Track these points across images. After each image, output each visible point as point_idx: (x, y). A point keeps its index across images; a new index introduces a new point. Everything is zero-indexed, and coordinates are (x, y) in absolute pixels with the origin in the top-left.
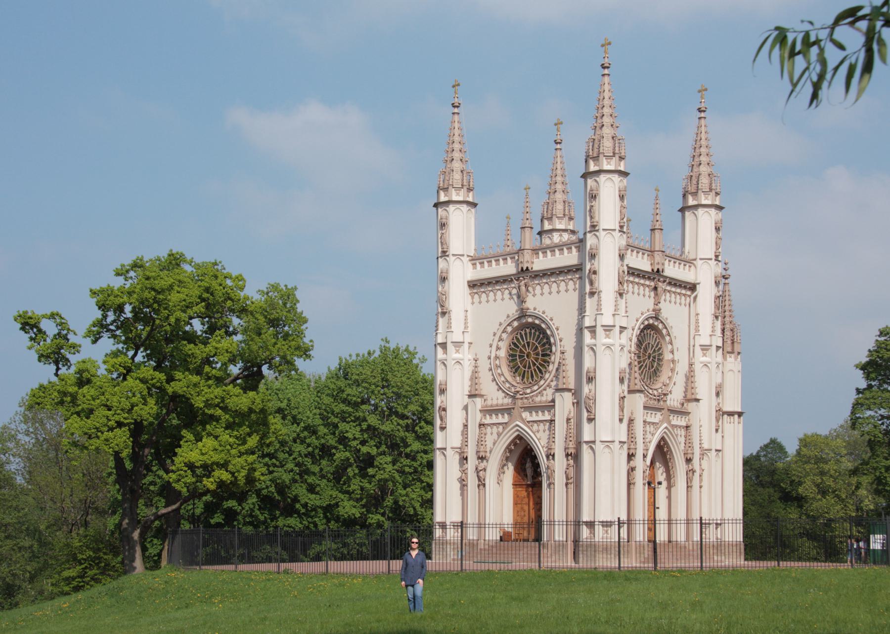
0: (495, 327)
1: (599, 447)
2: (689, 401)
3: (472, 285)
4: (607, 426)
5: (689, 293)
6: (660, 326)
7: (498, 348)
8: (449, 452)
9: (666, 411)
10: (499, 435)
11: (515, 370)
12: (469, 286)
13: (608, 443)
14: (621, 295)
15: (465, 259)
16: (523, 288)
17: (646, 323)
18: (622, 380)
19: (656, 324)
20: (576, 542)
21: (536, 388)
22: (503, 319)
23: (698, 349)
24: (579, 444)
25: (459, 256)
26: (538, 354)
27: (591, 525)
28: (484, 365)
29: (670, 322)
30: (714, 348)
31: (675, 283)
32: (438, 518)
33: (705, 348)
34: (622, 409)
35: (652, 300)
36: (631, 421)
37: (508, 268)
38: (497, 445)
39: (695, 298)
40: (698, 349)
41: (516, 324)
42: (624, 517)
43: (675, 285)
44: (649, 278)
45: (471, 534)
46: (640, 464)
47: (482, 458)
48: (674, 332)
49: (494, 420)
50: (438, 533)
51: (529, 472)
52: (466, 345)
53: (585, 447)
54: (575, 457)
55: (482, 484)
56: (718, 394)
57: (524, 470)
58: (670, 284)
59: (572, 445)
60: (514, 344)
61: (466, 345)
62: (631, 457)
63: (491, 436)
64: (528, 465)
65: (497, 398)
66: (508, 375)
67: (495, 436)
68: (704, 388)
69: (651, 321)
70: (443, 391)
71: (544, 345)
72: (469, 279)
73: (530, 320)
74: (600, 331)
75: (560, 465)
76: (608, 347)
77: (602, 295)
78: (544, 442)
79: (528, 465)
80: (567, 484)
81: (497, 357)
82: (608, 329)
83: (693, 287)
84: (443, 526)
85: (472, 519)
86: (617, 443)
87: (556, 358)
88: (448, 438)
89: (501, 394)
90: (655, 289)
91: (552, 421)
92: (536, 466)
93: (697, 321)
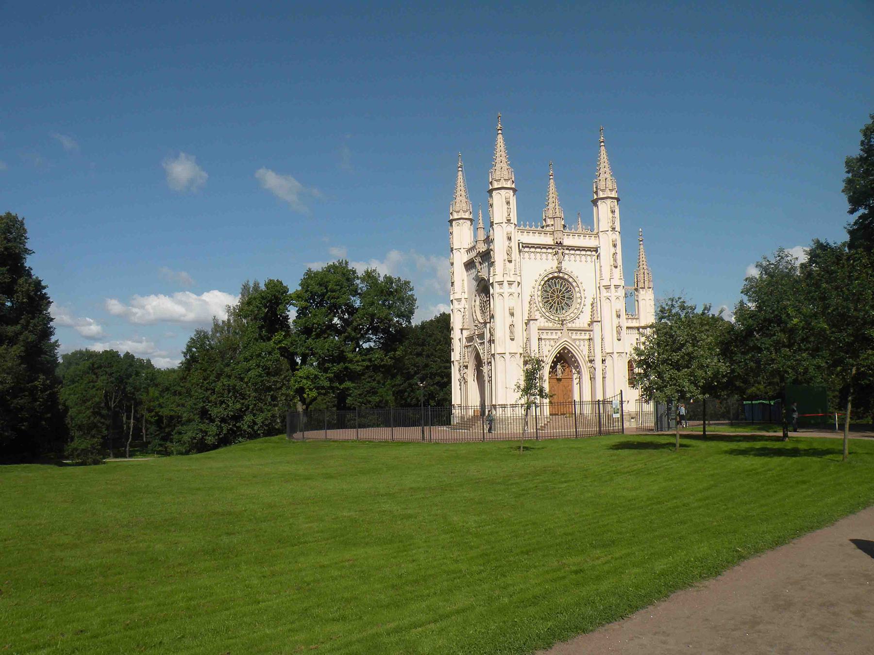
1: (497, 357)
5: (594, 253)
6: (566, 277)
8: (455, 363)
9: (565, 331)
17: (551, 276)
19: (561, 275)
23: (602, 288)
29: (574, 275)
33: (607, 287)
35: (556, 262)
40: (602, 288)
48: (580, 279)
52: (463, 300)
55: (466, 382)
69: (556, 275)
72: (465, 260)
74: (506, 284)
77: (496, 263)
82: (501, 283)
86: (507, 354)
88: (455, 356)
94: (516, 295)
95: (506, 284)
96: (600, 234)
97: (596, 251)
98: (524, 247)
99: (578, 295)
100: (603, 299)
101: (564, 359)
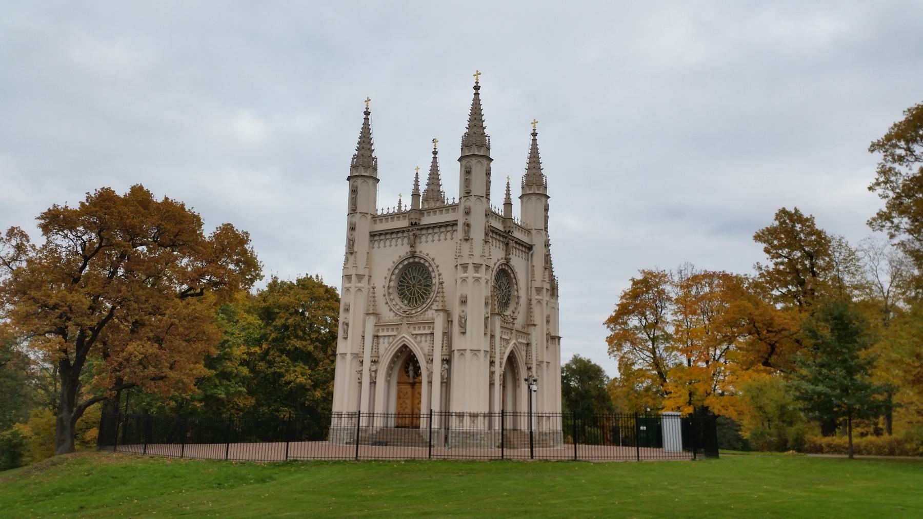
0: (390, 265)
1: (468, 354)
2: (528, 325)
3: (373, 235)
4: (474, 339)
7: (390, 281)
8: (349, 357)
10: (390, 344)
11: (402, 295)
12: (371, 236)
13: (475, 352)
14: (486, 242)
15: (369, 217)
16: (412, 237)
18: (486, 304)
20: (447, 429)
21: (419, 309)
22: (396, 259)
24: (451, 352)
25: (364, 214)
26: (421, 285)
27: (460, 415)
28: (380, 291)
30: (545, 290)
31: (519, 243)
32: (336, 408)
33: (539, 290)
34: (486, 327)
36: (492, 336)
37: (404, 223)
38: (387, 350)
39: (532, 255)
40: (533, 289)
41: (406, 263)
42: (487, 411)
43: (519, 244)
44: (503, 236)
45: (364, 423)
46: (498, 370)
47: (374, 362)
49: (385, 333)
50: (334, 421)
51: (411, 373)
53: (456, 355)
54: (447, 361)
55: (373, 383)
56: (548, 322)
57: (407, 372)
58: (516, 242)
59: (445, 352)
60: (404, 278)
61: (366, 278)
62: (492, 363)
63: (383, 345)
64: (411, 368)
65: (388, 316)
66: (398, 300)
67: (386, 345)
68: (538, 318)
70: (347, 310)
71: (426, 278)
73: (417, 260)
74: (471, 267)
75: (437, 368)
76: (477, 280)
78: (426, 351)
79: (411, 368)
80: (442, 383)
81: (389, 287)
82: (477, 267)
83: (530, 248)
84: (340, 415)
85: (364, 409)
86: (482, 352)
87: (435, 288)
89: (391, 314)
90: (507, 244)
91: (432, 334)
92: (417, 369)
93: (533, 271)
94: (470, 280)
95: (471, 267)
96: (534, 232)
97: (530, 248)
98: (494, 231)
99: (516, 293)
100: (534, 302)
101: (512, 361)
